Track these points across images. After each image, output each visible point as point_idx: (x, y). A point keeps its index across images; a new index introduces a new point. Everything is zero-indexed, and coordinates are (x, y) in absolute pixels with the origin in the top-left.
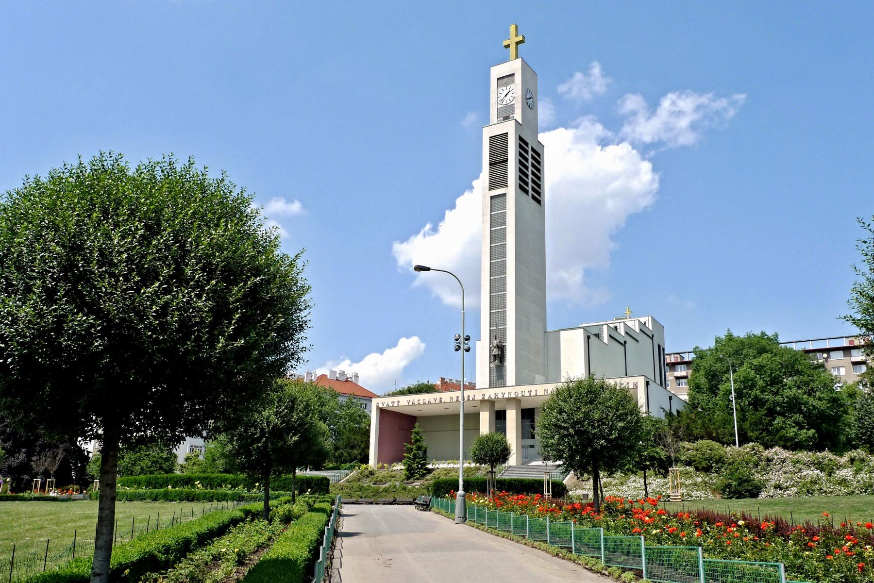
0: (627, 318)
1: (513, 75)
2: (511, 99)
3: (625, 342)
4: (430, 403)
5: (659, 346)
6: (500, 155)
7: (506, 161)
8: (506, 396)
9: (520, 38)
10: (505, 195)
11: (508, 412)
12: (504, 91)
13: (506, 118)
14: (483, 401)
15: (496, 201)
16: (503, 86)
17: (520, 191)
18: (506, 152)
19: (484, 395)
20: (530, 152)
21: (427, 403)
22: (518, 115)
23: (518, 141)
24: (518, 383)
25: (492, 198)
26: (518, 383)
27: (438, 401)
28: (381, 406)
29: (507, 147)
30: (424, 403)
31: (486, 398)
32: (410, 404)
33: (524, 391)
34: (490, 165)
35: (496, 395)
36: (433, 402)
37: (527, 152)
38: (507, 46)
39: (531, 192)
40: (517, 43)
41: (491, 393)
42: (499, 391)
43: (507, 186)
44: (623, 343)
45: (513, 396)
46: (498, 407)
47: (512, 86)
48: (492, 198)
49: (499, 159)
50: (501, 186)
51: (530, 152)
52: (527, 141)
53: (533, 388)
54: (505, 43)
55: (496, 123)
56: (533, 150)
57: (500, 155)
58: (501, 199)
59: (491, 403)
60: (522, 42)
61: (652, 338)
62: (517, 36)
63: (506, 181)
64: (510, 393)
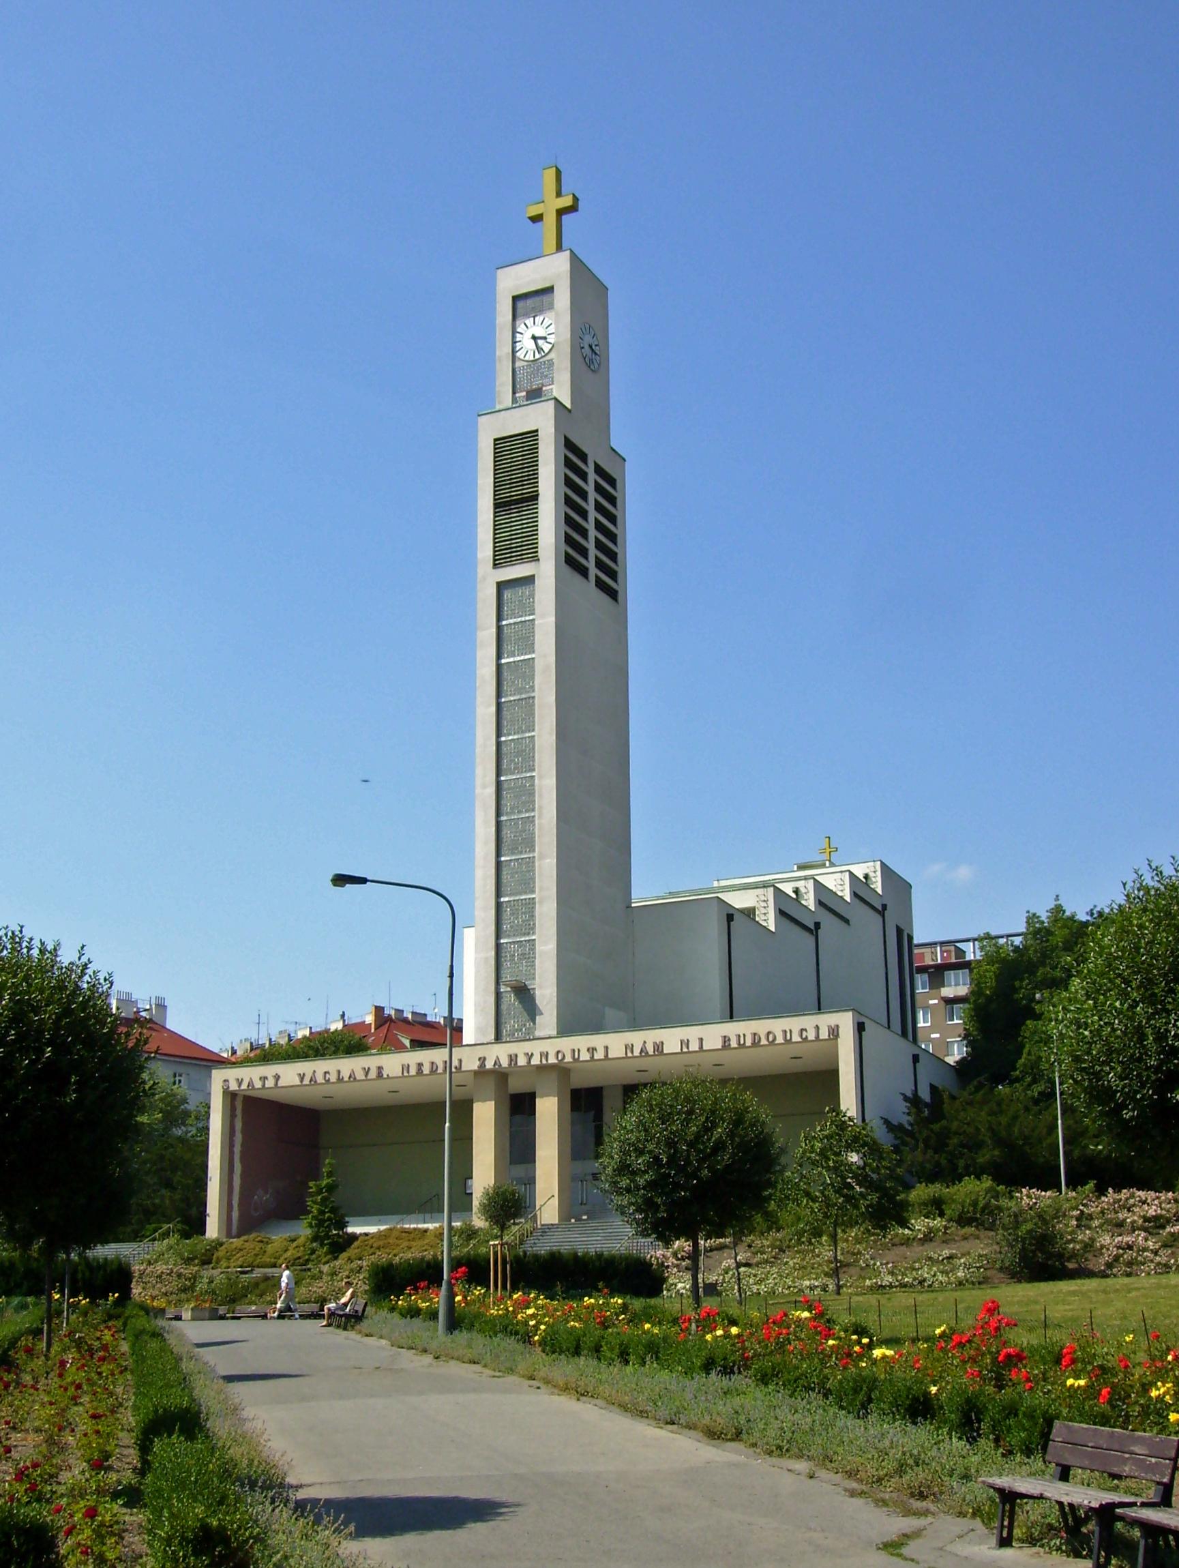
0: (823, 866)
3: (817, 925)
5: (899, 931)
6: (521, 482)
7: (535, 498)
8: (535, 1061)
9: (566, 201)
10: (533, 577)
11: (540, 1103)
12: (530, 328)
13: (535, 395)
14: (481, 1073)
16: (527, 315)
17: (567, 570)
18: (533, 477)
19: (483, 1060)
20: (592, 476)
21: (346, 1079)
22: (561, 389)
23: (563, 450)
27: (373, 1074)
28: (233, 1086)
33: (580, 1045)
34: (497, 506)
35: (513, 1058)
36: (360, 1075)
37: (583, 476)
38: (537, 219)
39: (593, 571)
40: (561, 212)
41: (499, 1054)
42: (520, 1049)
44: (812, 927)
45: (552, 1060)
46: (516, 1086)
48: (501, 586)
49: (516, 493)
50: (521, 559)
51: (592, 476)
52: (585, 449)
54: (534, 211)
55: (510, 404)
56: (599, 470)
59: (500, 1076)
60: (573, 209)
61: (882, 911)
62: (559, 194)
63: (534, 545)
64: (545, 1055)
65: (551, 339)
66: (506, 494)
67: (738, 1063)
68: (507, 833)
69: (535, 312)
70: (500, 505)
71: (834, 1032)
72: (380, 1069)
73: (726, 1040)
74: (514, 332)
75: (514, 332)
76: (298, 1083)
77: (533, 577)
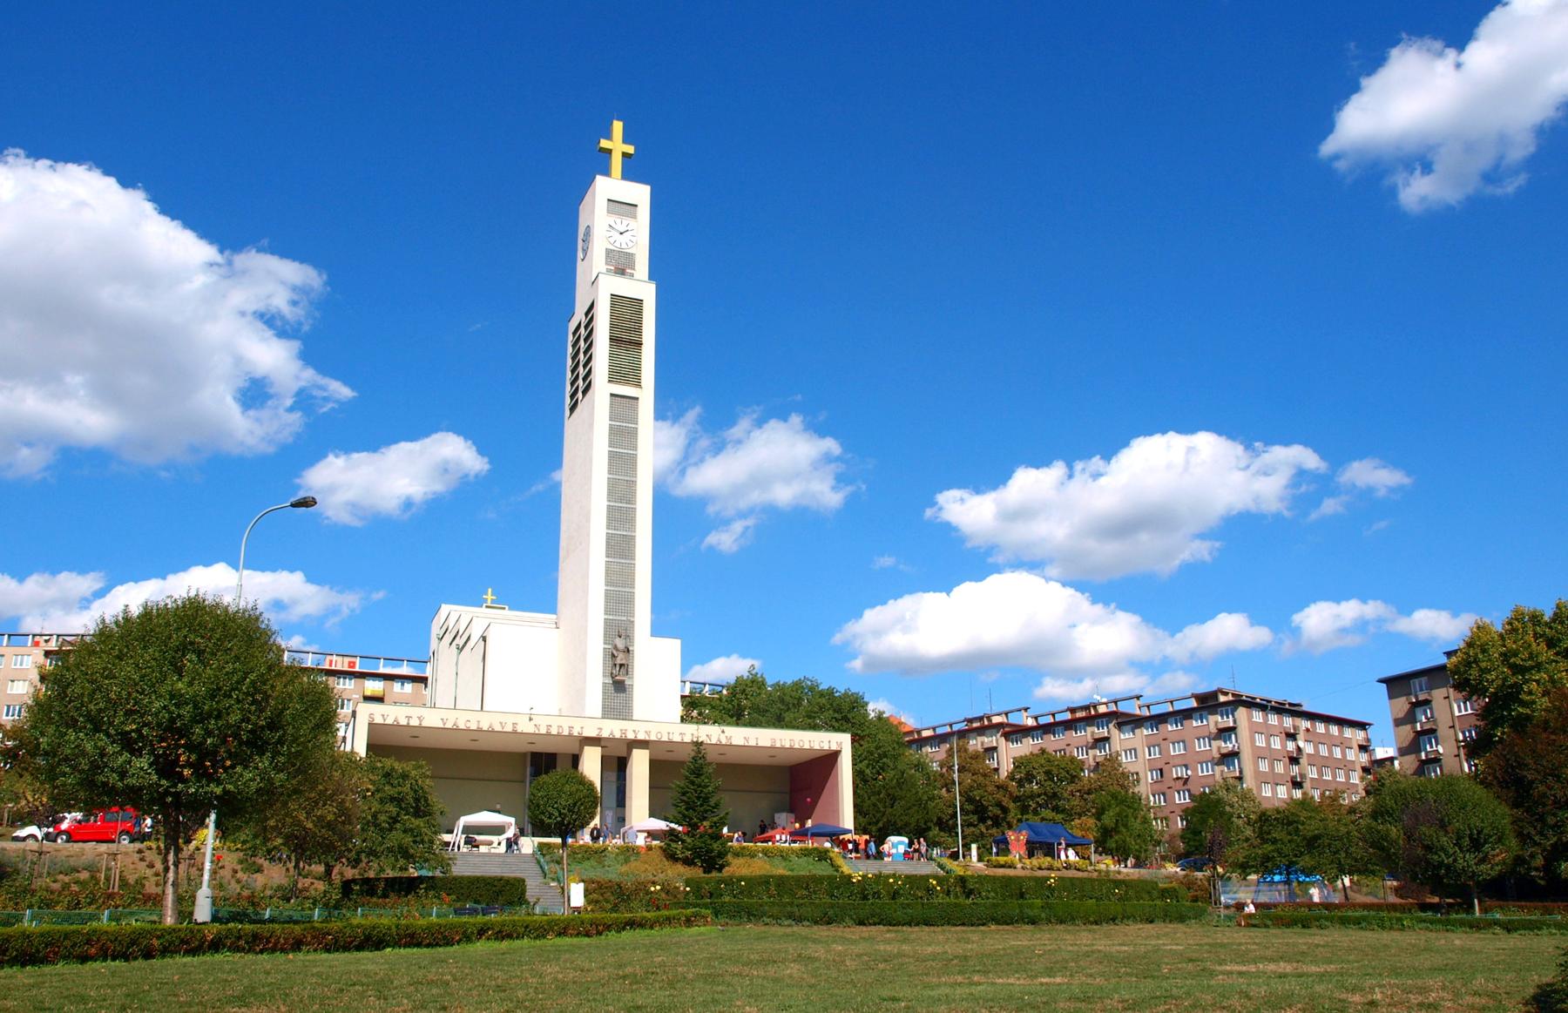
1: (636, 206)
2: (630, 244)
7: (640, 344)
8: (641, 737)
10: (637, 399)
18: (638, 330)
25: (612, 395)
28: (379, 720)
29: (640, 322)
31: (605, 734)
38: (609, 152)
43: (638, 385)
45: (653, 738)
47: (632, 224)
49: (625, 336)
50: (627, 382)
54: (604, 143)
57: (629, 330)
70: (614, 340)
72: (514, 724)
76: (442, 726)
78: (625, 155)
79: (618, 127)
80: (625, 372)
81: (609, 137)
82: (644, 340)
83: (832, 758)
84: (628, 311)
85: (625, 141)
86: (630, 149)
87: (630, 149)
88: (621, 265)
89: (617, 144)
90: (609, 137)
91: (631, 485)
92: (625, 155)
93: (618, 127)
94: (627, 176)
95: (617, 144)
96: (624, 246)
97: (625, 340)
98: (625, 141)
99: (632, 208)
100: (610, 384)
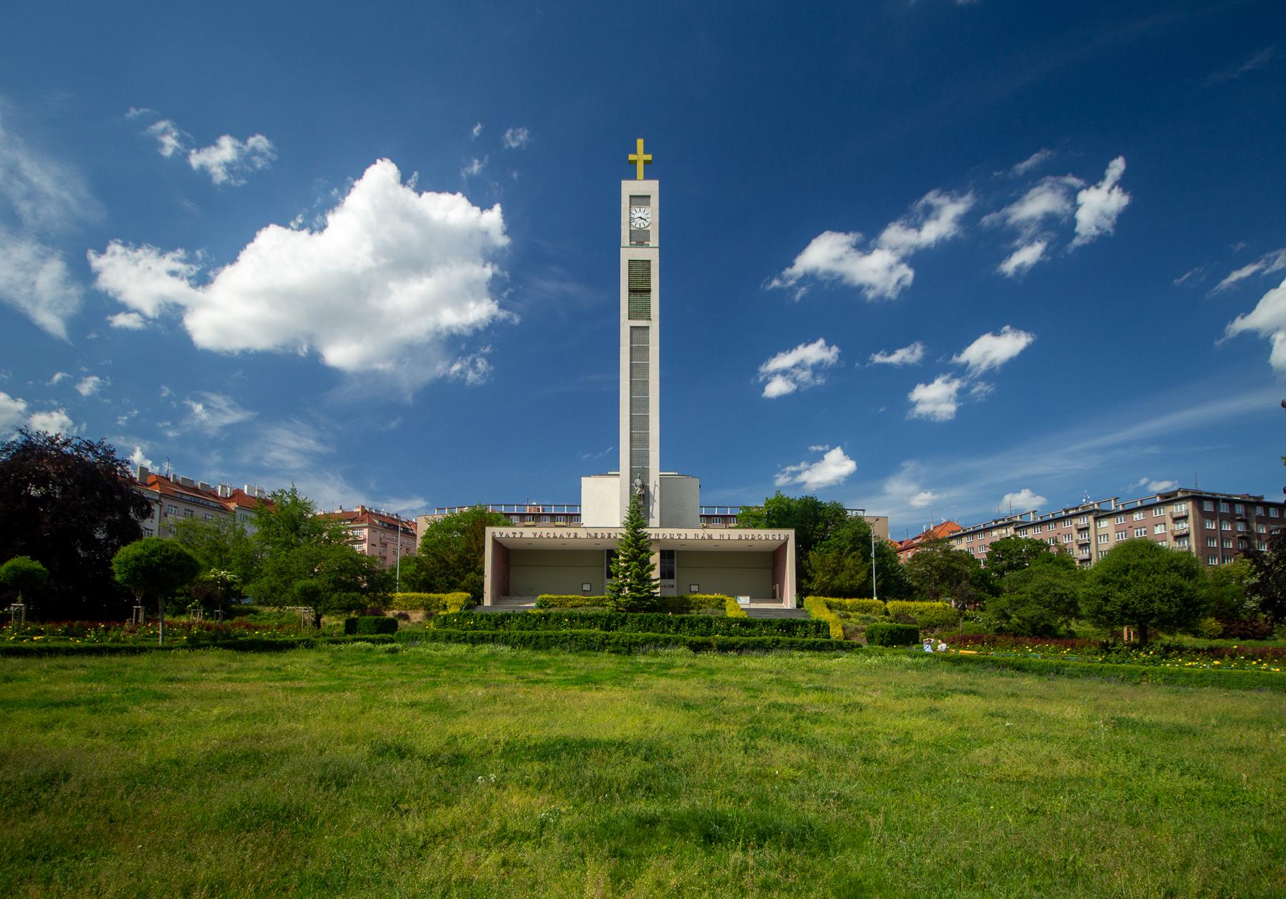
1: (649, 196)
4: (561, 537)
7: (649, 291)
10: (648, 327)
12: (638, 213)
15: (635, 332)
24: (662, 526)
26: (662, 526)
29: (649, 276)
30: (555, 537)
32: (537, 536)
33: (668, 533)
36: (565, 536)
38: (635, 162)
47: (648, 210)
49: (640, 287)
50: (642, 318)
53: (683, 532)
54: (631, 157)
58: (641, 332)
65: (649, 220)
66: (634, 287)
67: (742, 546)
68: (636, 436)
69: (640, 205)
70: (632, 291)
71: (787, 539)
73: (740, 536)
74: (630, 213)
75: (630, 213)
77: (648, 327)
78: (646, 162)
79: (640, 142)
80: (639, 311)
81: (635, 152)
82: (652, 288)
83: (784, 546)
84: (639, 268)
85: (646, 152)
86: (649, 157)
87: (649, 157)
88: (639, 238)
89: (640, 156)
90: (635, 152)
91: (646, 383)
92: (646, 162)
93: (640, 142)
94: (647, 177)
95: (640, 156)
96: (642, 226)
97: (638, 291)
98: (646, 152)
99: (646, 200)
100: (631, 321)
